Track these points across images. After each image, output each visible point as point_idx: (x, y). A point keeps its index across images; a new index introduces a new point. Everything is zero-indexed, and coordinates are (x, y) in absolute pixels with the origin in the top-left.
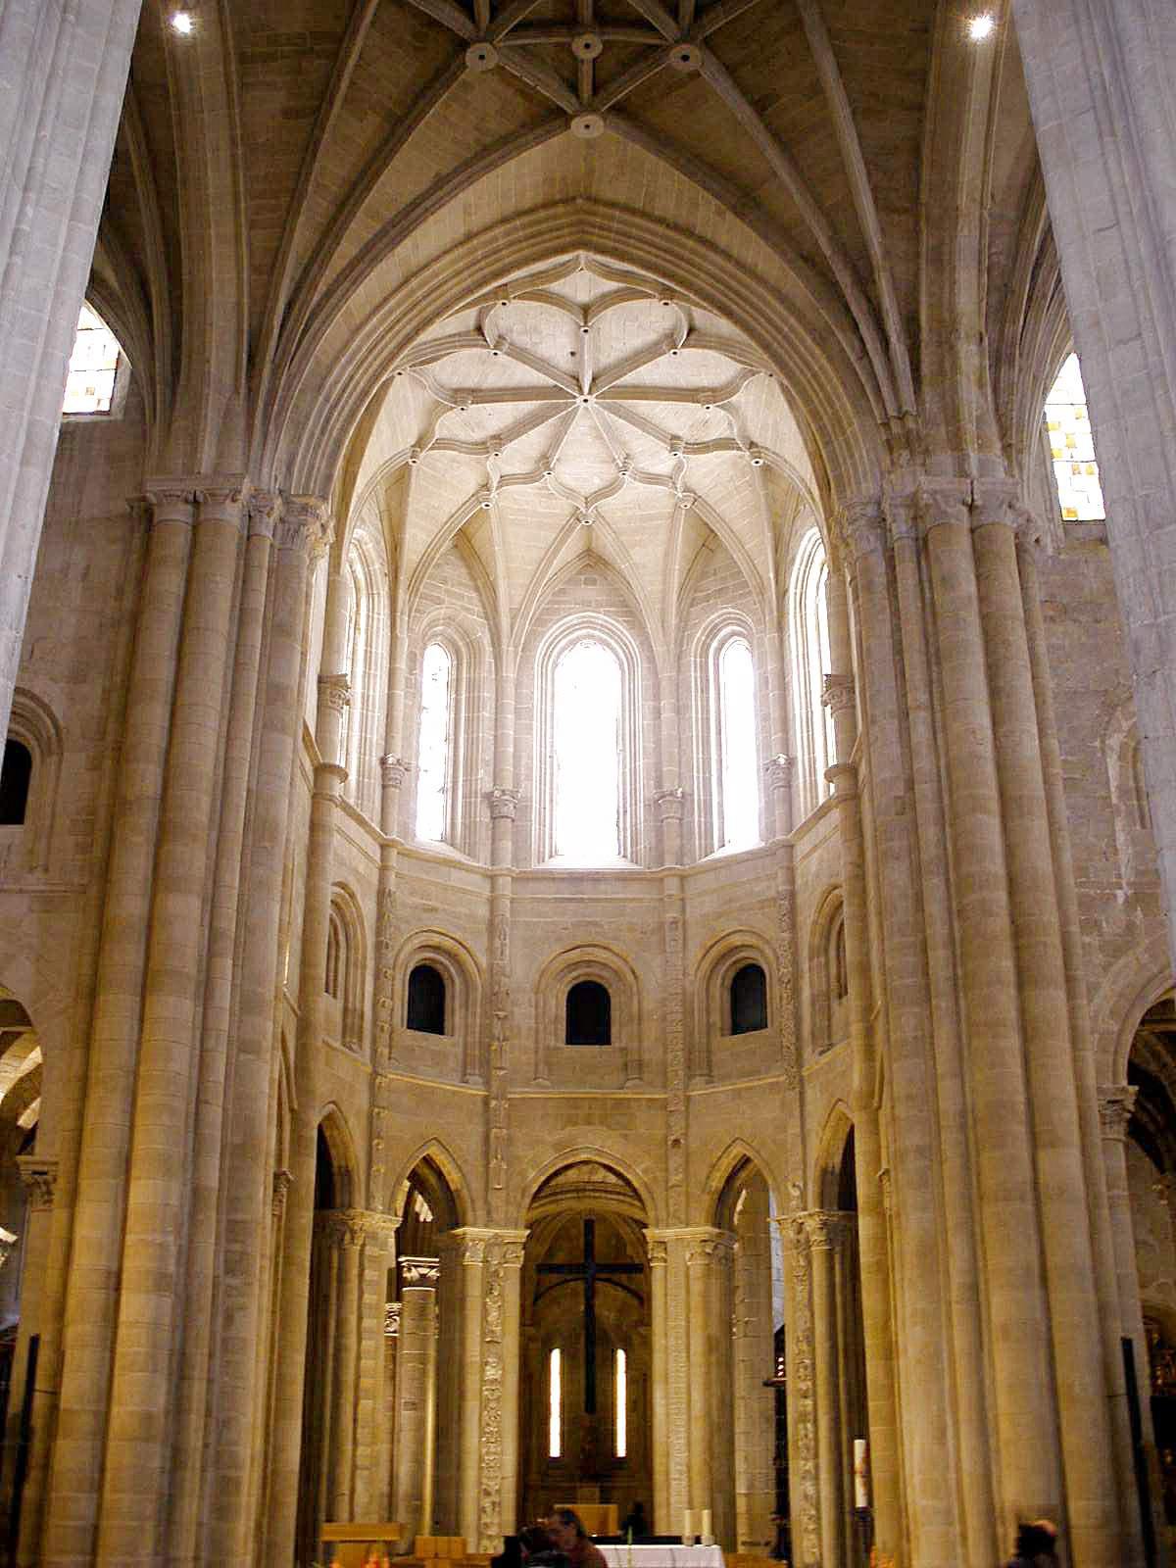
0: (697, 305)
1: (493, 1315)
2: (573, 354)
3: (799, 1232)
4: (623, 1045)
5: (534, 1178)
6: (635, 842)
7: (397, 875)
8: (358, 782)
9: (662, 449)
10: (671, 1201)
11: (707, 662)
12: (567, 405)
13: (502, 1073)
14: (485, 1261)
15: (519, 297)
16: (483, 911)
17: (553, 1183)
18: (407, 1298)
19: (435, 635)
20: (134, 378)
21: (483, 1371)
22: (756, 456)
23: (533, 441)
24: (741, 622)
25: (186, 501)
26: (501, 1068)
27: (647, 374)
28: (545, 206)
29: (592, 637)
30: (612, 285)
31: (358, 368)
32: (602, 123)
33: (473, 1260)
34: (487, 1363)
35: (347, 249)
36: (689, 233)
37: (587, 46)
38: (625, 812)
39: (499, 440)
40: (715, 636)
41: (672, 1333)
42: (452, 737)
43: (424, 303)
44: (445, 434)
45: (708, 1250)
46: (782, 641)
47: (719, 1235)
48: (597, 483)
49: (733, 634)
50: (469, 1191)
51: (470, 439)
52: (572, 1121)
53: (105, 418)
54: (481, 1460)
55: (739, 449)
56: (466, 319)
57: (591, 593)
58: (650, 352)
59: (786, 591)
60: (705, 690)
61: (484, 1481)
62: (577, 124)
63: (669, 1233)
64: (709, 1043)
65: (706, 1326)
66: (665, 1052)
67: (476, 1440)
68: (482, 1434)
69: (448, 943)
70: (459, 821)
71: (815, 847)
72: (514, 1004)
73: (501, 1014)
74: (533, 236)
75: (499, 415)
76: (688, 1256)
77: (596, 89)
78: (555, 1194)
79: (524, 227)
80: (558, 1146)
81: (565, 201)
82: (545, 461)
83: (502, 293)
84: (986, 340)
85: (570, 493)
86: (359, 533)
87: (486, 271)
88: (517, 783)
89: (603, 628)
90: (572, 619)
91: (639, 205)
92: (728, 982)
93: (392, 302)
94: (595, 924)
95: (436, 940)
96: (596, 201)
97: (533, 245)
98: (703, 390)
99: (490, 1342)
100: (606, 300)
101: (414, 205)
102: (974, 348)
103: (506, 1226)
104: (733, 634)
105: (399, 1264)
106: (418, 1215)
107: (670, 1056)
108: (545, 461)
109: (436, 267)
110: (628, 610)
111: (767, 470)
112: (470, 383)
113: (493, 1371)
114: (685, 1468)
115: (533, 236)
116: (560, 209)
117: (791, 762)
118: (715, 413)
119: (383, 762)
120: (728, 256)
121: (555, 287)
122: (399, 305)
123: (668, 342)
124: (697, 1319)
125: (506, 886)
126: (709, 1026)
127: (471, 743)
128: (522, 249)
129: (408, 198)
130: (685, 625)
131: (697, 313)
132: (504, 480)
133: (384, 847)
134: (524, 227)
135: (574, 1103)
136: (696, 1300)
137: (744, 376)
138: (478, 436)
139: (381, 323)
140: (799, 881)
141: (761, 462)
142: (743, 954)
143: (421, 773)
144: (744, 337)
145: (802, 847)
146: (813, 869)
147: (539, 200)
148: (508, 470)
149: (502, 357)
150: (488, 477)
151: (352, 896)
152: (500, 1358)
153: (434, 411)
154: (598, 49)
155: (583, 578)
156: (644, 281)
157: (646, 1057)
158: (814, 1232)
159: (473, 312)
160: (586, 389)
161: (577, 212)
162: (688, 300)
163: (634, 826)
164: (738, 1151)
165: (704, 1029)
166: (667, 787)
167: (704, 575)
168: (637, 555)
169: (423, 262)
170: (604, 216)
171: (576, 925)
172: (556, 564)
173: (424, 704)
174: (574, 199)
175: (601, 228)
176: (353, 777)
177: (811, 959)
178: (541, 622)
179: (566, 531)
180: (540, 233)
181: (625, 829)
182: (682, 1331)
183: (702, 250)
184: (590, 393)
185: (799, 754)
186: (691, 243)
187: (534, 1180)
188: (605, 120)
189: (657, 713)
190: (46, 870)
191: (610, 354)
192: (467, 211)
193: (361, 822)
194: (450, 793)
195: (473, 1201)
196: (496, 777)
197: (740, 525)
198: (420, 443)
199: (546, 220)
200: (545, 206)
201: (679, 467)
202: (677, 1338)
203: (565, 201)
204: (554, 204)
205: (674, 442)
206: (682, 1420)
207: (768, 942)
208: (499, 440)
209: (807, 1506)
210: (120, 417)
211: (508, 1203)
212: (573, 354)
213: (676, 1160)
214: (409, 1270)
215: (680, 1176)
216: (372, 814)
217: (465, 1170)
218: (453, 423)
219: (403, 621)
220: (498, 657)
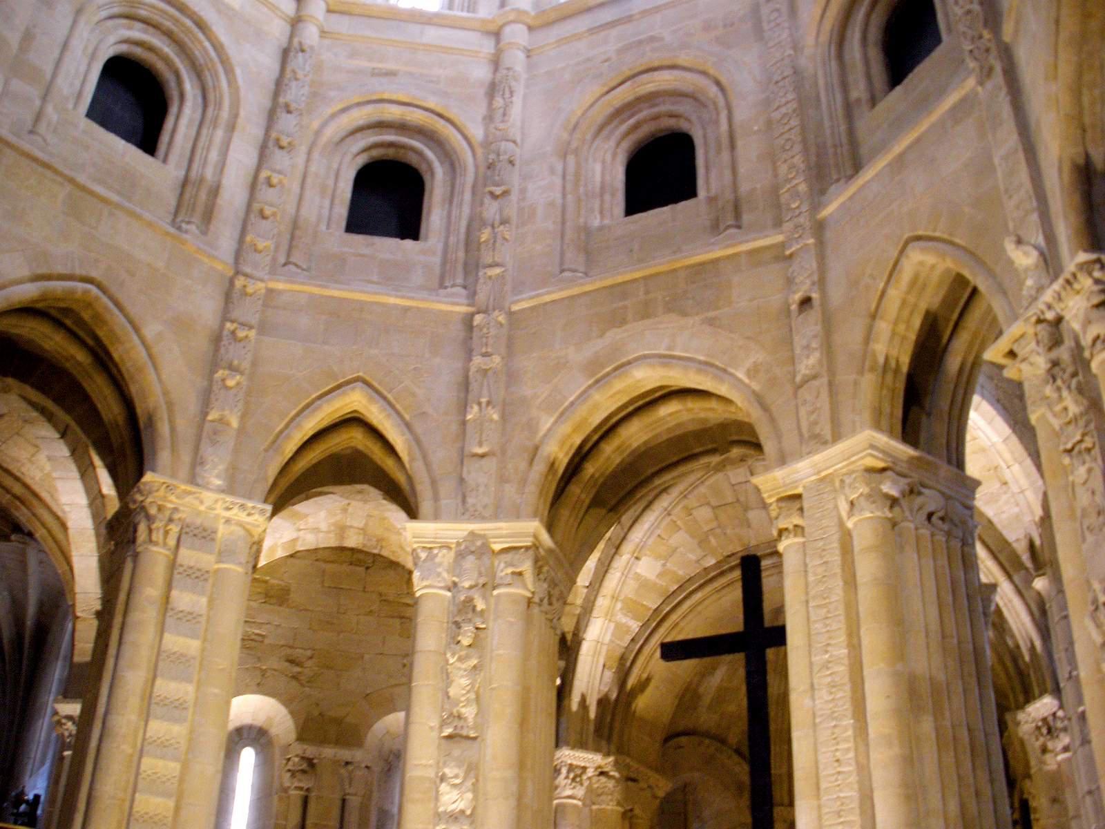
3: (1056, 342)
4: (713, 192)
7: (323, 33)
10: (803, 412)
34: (443, 779)
41: (822, 680)
45: (890, 488)
50: (427, 464)
52: (618, 320)
64: (851, 132)
65: (899, 650)
66: (775, 169)
69: (416, 117)
72: (525, 177)
73: (498, 190)
76: (844, 507)
92: (875, 33)
94: (652, 39)
95: (393, 113)
103: (495, 517)
107: (783, 169)
113: (454, 794)
124: (874, 639)
125: (517, 35)
135: (621, 291)
136: (868, 597)
151: (201, 25)
152: (472, 769)
165: (840, 112)
171: (620, 51)
182: (842, 669)
195: (434, 483)
211: (502, 479)
213: (808, 329)
215: (813, 359)
217: (419, 428)
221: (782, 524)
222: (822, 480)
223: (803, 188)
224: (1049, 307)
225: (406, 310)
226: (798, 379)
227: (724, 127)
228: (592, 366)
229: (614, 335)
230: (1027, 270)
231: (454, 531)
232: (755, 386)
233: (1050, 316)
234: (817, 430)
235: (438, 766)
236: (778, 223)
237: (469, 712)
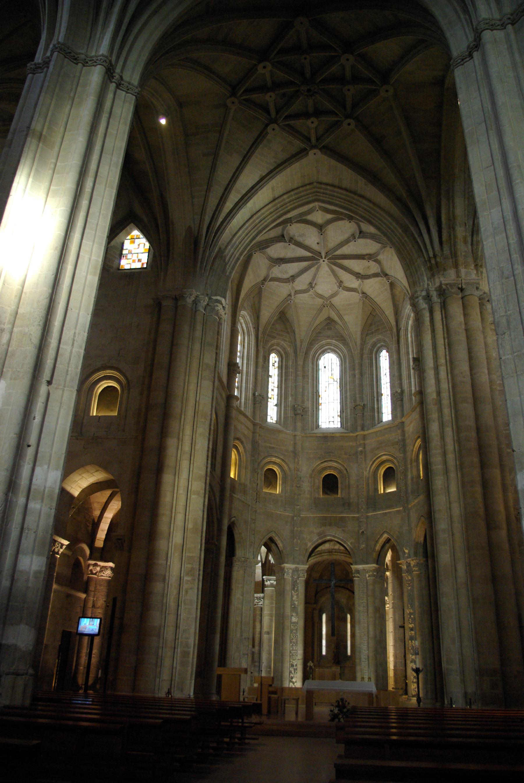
0: (361, 221)
1: (295, 598)
2: (318, 243)
5: (310, 546)
6: (346, 423)
8: (245, 402)
9: (353, 278)
11: (372, 357)
12: (317, 263)
13: (299, 507)
14: (292, 577)
15: (296, 222)
16: (291, 448)
17: (318, 549)
18: (266, 592)
19: (273, 350)
20: (154, 256)
21: (291, 618)
22: (388, 279)
23: (306, 277)
24: (385, 341)
25: (173, 299)
26: (298, 505)
27: (346, 250)
28: (302, 187)
29: (330, 349)
30: (329, 216)
31: (235, 250)
32: (320, 152)
33: (288, 577)
34: (292, 616)
35: (229, 205)
36: (355, 193)
37: (312, 122)
39: (293, 278)
40: (375, 347)
42: (280, 386)
43: (259, 225)
44: (273, 276)
46: (399, 347)
47: (379, 568)
48: (330, 292)
49: (382, 346)
51: (283, 278)
53: (146, 270)
54: (290, 652)
55: (382, 277)
56: (278, 231)
57: (329, 333)
58: (346, 242)
59: (400, 329)
60: (371, 367)
61: (291, 660)
62: (311, 153)
63: (360, 567)
67: (289, 645)
68: (291, 642)
70: (283, 416)
71: (411, 422)
72: (303, 482)
74: (299, 198)
75: (293, 268)
76: (367, 575)
77: (317, 139)
78: (321, 553)
79: (294, 195)
80: (319, 534)
81: (309, 184)
82: (311, 285)
83: (289, 221)
84: (467, 224)
85: (321, 296)
86: (243, 312)
87: (281, 212)
88: (303, 402)
89: (335, 346)
90: (324, 342)
91: (337, 183)
93: (247, 225)
96: (321, 183)
97: (299, 201)
98: (367, 255)
99: (294, 608)
100: (329, 222)
101: (252, 188)
102: (463, 229)
104: (382, 346)
105: (263, 579)
106: (270, 561)
108: (311, 285)
109: (263, 211)
110: (342, 339)
111: (392, 285)
112: (282, 256)
113: (295, 619)
114: (367, 657)
115: (299, 198)
116: (308, 187)
117: (402, 392)
118: (372, 263)
119: (254, 394)
120: (369, 201)
121: (309, 217)
122: (249, 226)
123: (353, 237)
127: (286, 388)
128: (295, 203)
129: (250, 185)
130: (363, 343)
131: (362, 224)
132: (297, 292)
133: (255, 425)
134: (294, 195)
137: (381, 249)
138: (286, 276)
139: (243, 233)
140: (407, 436)
141: (390, 281)
143: (269, 400)
144: (379, 233)
145: (407, 422)
146: (411, 430)
147: (300, 185)
148: (297, 288)
149: (292, 246)
150: (291, 292)
152: (297, 614)
153: (270, 268)
154: (316, 123)
155: (327, 327)
156: (341, 213)
158: (414, 566)
159: (280, 228)
160: (323, 257)
161: (314, 188)
162: (358, 220)
163: (346, 416)
164: (386, 536)
166: (358, 402)
167: (371, 325)
168: (346, 318)
169: (258, 209)
170: (324, 189)
172: (317, 322)
173: (270, 374)
174: (313, 183)
175: (323, 193)
176: (243, 400)
178: (311, 344)
179: (320, 310)
180: (302, 197)
181: (343, 418)
183: (361, 199)
184: (325, 258)
185: (406, 387)
186: (356, 197)
187: (310, 546)
188: (321, 151)
189: (354, 375)
190: (124, 431)
191: (331, 245)
192: (273, 189)
193: (246, 416)
194: (279, 406)
196: (296, 400)
197: (383, 306)
198: (265, 280)
199: (303, 191)
200: (302, 187)
201: (360, 285)
202: (363, 606)
203: (309, 184)
204: (305, 185)
205: (358, 276)
206: (365, 639)
207: (395, 458)
208: (293, 278)
209: (413, 673)
210: (150, 269)
212: (318, 243)
214: (267, 581)
216: (249, 413)
218: (277, 271)
219: (261, 345)
220: (296, 356)
221: (355, 575)
225: (281, 514)
227: (347, 483)
228: (319, 534)
229: (323, 528)
231: (293, 566)
232: (351, 546)
235: (291, 613)
236: (358, 512)
237: (296, 603)
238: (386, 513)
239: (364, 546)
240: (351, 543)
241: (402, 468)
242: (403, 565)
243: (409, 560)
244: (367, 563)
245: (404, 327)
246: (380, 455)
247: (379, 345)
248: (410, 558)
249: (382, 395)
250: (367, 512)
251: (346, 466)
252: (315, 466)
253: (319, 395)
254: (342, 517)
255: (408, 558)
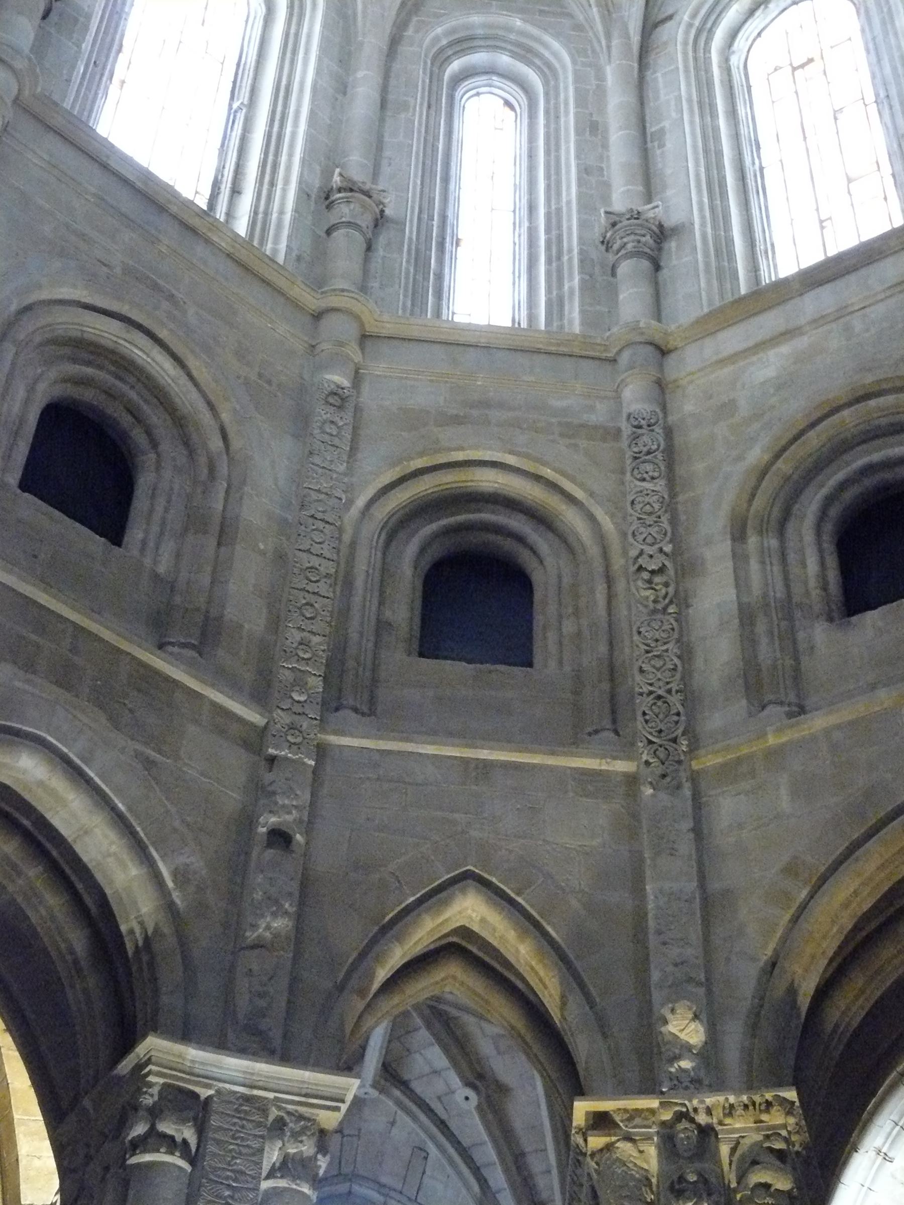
38: (236, 191)
49: (490, 71)
66: (275, 623)
76: (272, 1155)
126: (382, 626)
142: (487, 516)
157: (231, 613)
177: (739, 534)
222: (248, 1099)
223: (316, 684)
224: (709, 1112)
226: (251, 936)
230: (687, 1048)
232: (177, 897)
233: (702, 1119)
234: (264, 1024)
238: (486, 766)
239: (281, 924)
240: (181, 876)
241: (649, 550)
242: (629, 1138)
243: (709, 1101)
244: (285, 1059)
245: (694, 16)
246: (460, 456)
247: (479, 58)
248: (718, 1086)
249: (457, 245)
250: (322, 724)
251: (225, 416)
252: (45, 295)
253: (121, 46)
254: (157, 672)
255: (696, 1084)
